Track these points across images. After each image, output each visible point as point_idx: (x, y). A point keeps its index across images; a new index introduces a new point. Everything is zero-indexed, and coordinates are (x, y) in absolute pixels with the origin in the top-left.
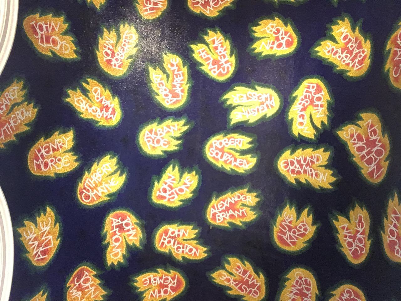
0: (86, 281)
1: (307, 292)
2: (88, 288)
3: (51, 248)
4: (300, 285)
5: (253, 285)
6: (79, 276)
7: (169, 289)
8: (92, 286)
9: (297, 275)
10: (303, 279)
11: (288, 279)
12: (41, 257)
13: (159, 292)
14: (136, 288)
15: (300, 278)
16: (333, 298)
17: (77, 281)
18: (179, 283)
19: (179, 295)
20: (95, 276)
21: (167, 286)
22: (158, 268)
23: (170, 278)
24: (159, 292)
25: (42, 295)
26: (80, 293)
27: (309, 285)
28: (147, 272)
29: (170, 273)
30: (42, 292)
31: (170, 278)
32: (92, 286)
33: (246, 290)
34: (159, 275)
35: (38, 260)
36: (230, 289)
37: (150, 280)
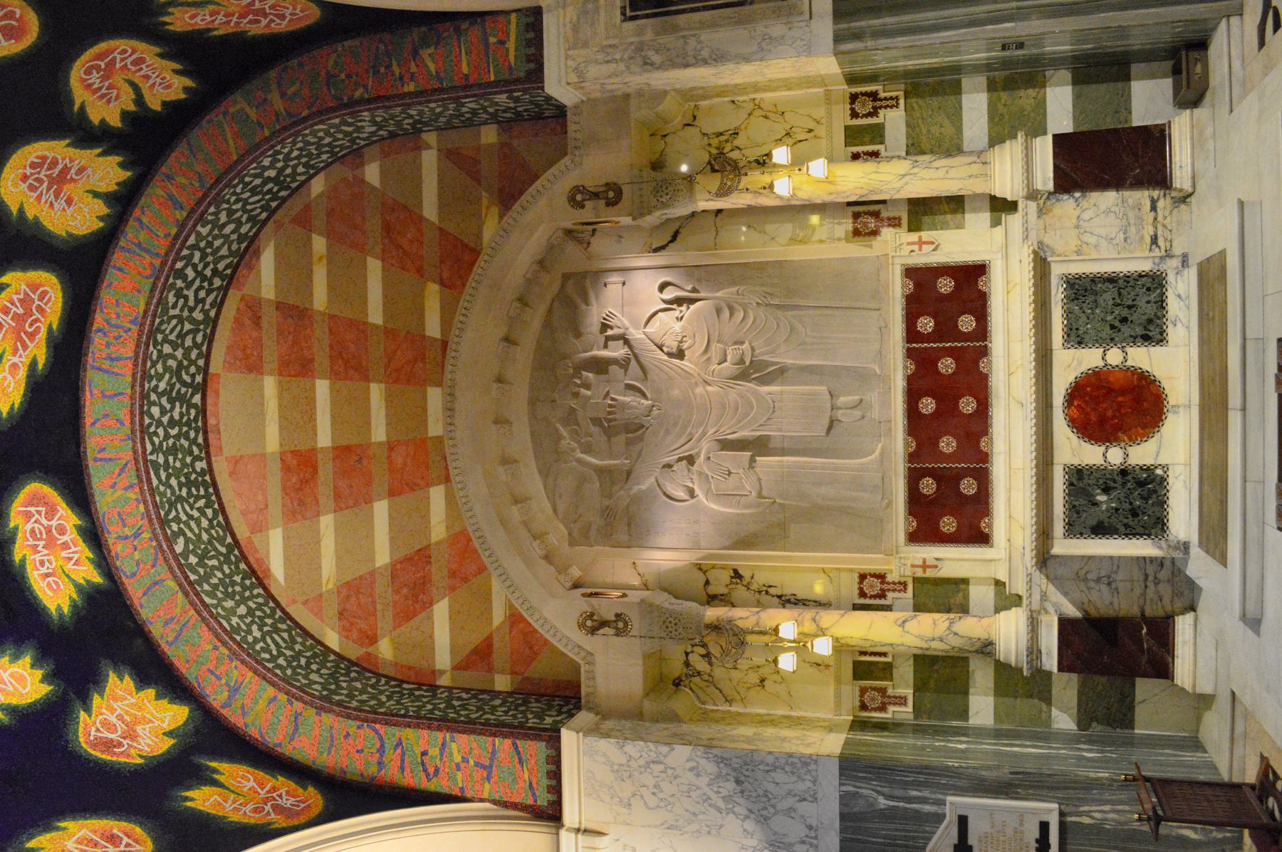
0: (108, 725)
1: (60, 167)
2: (120, 718)
3: (95, 832)
4: (40, 181)
5: (26, 301)
6: (109, 745)
7: (54, 523)
8: (112, 710)
9: (15, 185)
10: (28, 171)
11: (21, 211)
12: (126, 840)
13: (65, 546)
14: (74, 606)
15: (25, 178)
16: (89, 110)
17: (120, 745)
18: (34, 500)
19: (62, 494)
20: (88, 710)
21: (48, 529)
22: (12, 561)
23: (29, 526)
24: (65, 546)
25: (192, 800)
26: (139, 729)
27: (44, 158)
28: (29, 588)
29: (16, 528)
30: (189, 804)
31: (29, 526)
32: (112, 710)
33: (37, 320)
34: (30, 557)
35: (137, 841)
36: (34, 363)
37: (47, 575)
